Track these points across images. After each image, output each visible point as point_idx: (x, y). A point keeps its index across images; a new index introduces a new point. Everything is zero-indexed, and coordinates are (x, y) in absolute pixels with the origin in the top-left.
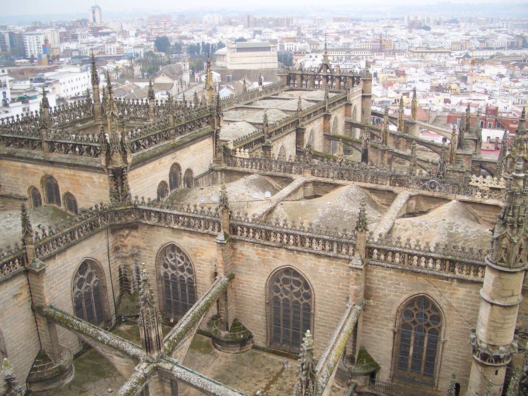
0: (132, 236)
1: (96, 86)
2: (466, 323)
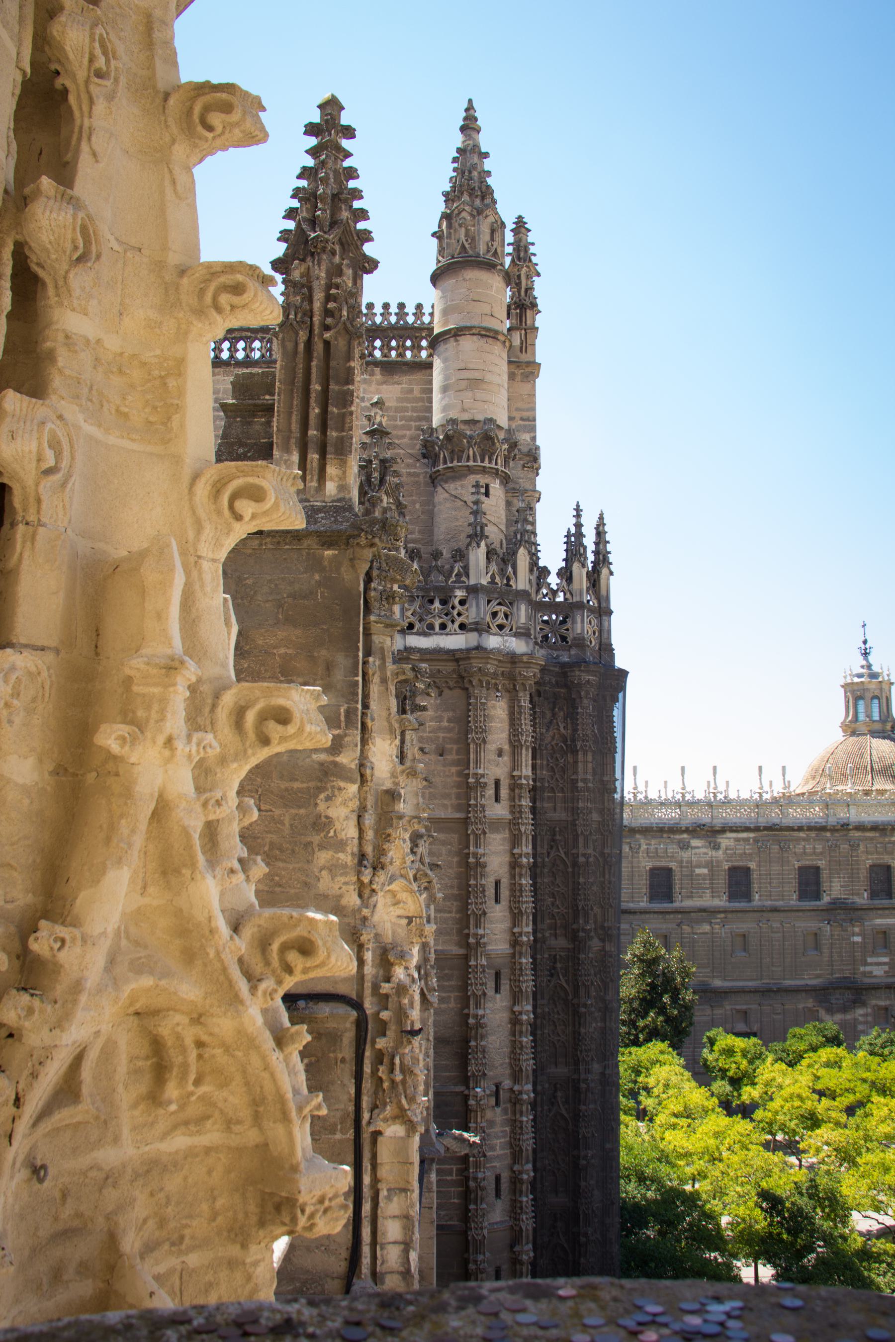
2: (410, 461)
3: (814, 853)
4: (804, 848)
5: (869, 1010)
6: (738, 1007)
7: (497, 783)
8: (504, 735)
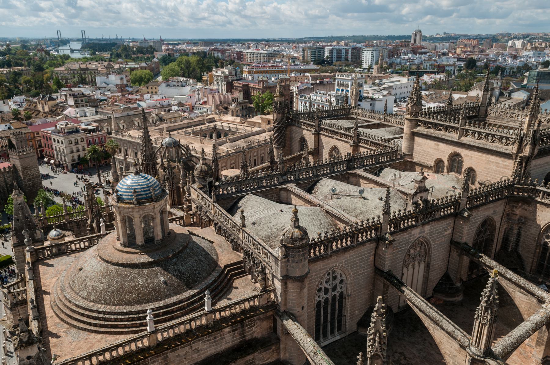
0: (523, 209)
1: (485, 93)
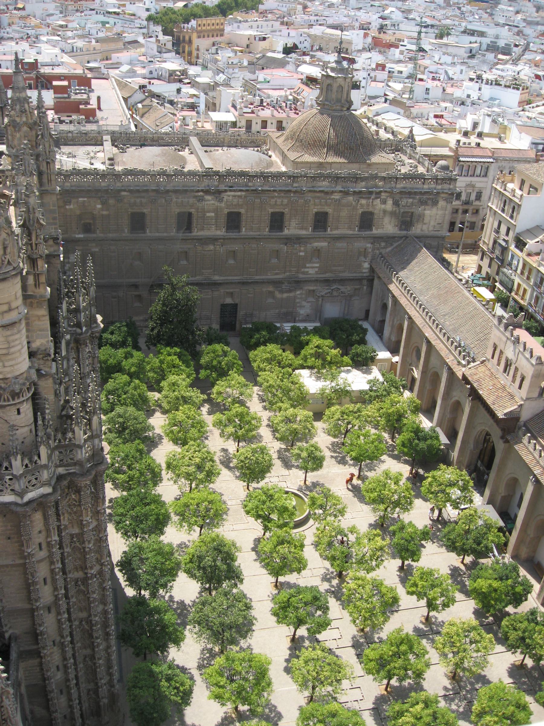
3: (282, 205)
4: (276, 201)
5: (304, 292)
6: (228, 291)
7: (40, 544)
8: (42, 524)
